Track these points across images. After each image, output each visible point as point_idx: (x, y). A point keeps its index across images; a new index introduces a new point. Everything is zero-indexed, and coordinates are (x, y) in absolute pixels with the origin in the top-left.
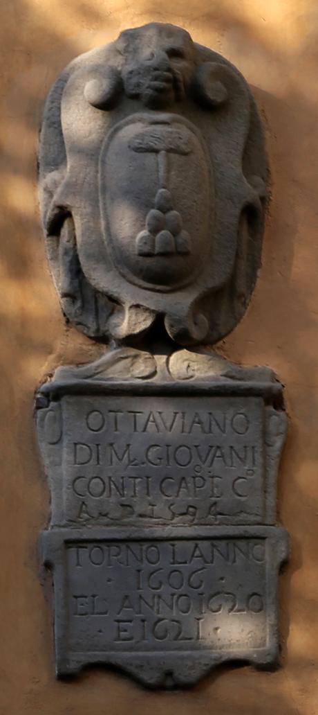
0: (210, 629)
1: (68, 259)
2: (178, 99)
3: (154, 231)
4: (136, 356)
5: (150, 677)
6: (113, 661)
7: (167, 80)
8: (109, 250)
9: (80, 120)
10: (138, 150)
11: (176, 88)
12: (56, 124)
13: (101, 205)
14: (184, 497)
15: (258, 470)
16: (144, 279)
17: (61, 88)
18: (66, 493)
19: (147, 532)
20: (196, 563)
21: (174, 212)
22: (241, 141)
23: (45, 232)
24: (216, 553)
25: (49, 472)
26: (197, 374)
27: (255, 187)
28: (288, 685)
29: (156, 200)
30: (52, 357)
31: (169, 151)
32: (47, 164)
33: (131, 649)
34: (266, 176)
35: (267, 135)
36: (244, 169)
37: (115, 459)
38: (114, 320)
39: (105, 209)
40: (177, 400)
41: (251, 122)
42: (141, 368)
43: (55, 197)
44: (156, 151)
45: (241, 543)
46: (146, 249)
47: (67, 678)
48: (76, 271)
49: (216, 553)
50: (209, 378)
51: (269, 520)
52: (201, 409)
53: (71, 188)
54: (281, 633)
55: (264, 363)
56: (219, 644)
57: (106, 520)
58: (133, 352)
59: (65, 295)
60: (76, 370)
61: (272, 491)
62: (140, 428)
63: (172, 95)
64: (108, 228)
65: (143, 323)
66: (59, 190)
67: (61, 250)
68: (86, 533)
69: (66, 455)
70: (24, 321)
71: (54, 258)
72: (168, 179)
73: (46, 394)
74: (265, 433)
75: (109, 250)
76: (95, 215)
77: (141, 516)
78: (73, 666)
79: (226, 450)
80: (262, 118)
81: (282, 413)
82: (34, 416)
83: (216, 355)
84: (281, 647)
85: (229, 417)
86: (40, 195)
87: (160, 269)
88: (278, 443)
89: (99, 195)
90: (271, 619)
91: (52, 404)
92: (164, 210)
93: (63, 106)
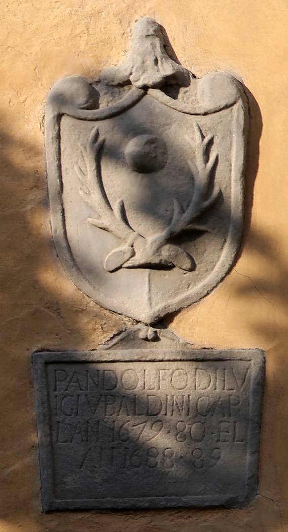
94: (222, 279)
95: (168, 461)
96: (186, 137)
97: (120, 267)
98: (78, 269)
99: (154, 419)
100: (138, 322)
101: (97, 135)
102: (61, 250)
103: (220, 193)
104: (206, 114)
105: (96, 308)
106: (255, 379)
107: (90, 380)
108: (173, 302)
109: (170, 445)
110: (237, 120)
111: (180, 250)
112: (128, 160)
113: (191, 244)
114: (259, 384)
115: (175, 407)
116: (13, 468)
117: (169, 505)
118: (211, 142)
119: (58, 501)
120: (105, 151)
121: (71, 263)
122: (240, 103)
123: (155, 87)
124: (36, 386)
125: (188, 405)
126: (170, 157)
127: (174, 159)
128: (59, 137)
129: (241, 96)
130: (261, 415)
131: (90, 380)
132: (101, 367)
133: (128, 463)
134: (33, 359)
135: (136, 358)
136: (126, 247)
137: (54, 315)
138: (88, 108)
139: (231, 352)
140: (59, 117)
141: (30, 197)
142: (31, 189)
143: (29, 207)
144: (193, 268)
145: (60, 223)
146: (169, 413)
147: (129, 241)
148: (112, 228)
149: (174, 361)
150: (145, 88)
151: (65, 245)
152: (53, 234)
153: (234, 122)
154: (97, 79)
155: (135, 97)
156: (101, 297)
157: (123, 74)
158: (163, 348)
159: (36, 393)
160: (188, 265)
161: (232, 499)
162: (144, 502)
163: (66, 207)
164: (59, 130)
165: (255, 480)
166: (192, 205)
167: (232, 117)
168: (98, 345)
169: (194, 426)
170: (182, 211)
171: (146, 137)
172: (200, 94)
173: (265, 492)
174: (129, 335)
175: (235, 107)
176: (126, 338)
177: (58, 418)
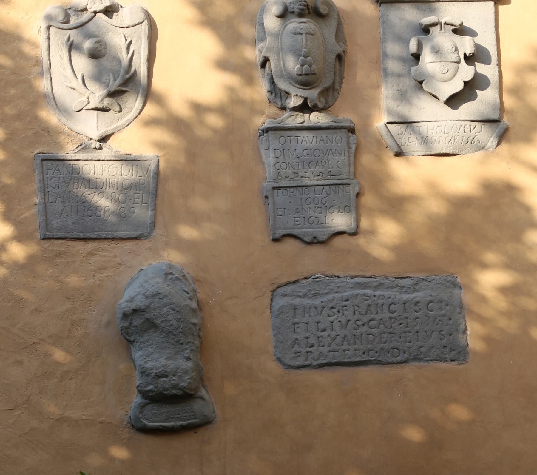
0: (330, 220)
1: (269, 77)
2: (309, 13)
3: (302, 65)
4: (297, 115)
5: (308, 239)
6: (293, 233)
7: (305, 6)
8: (285, 74)
9: (271, 22)
10: (295, 33)
11: (308, 9)
12: (262, 24)
13: (281, 55)
14: (318, 169)
15: (346, 158)
16: (299, 84)
17: (263, 10)
18: (272, 169)
19: (304, 183)
20: (324, 195)
21: (310, 58)
22: (335, 29)
23: (260, 67)
24: (331, 191)
25: (265, 161)
26: (321, 121)
27: (341, 47)
28: (361, 240)
29: (302, 53)
30: (264, 116)
31: (307, 33)
32: (259, 40)
33: (300, 228)
34: (345, 42)
35: (345, 26)
36: (336, 40)
37: (290, 155)
38: (288, 101)
39: (282, 57)
40: (314, 131)
41: (338, 21)
42: (299, 119)
43: (263, 53)
44: (302, 34)
45: (341, 187)
46: (299, 73)
47: (276, 240)
48: (272, 82)
49: (331, 191)
50: (325, 123)
51: (351, 177)
52: (323, 134)
53: (269, 49)
54: (358, 221)
55: (347, 116)
56: (334, 225)
57: (288, 179)
58: (296, 113)
59: (268, 92)
60: (274, 121)
61: (352, 166)
62: (300, 143)
63: (307, 11)
64: (284, 65)
65: (300, 102)
66: (264, 50)
67: (266, 74)
68: (281, 184)
69: (271, 154)
70: (253, 102)
71: (263, 77)
72: (306, 45)
73: (263, 131)
74: (348, 143)
75: (285, 74)
76: (279, 60)
77: (301, 177)
78: (278, 236)
79: (333, 150)
80: (342, 20)
81: (355, 136)
82: (258, 139)
83: (328, 114)
84: (358, 226)
85: (334, 137)
86: (257, 52)
87: (305, 81)
88: (354, 147)
89: (280, 51)
90: (354, 215)
91: (265, 134)
92: (305, 57)
93: (264, 17)
94: (136, 117)
95: (107, 213)
96: (116, 40)
97: (82, 110)
98: (59, 110)
99: (100, 191)
100: (91, 139)
101: (69, 37)
102: (50, 99)
103: (135, 71)
104: (127, 27)
105: (69, 131)
106: (153, 171)
107: (66, 170)
108: (109, 129)
109: (108, 205)
110: (145, 31)
111: (114, 101)
112: (86, 52)
113: (119, 97)
114: (155, 174)
115: (111, 185)
116: (24, 215)
117: (107, 237)
118: (130, 43)
119: (48, 233)
120: (73, 46)
121: (55, 107)
122: (146, 22)
123: (100, 12)
124: (37, 172)
125: (118, 184)
126: (108, 50)
127: (110, 51)
128: (49, 38)
129: (147, 18)
130: (156, 190)
131: (66, 170)
132: (71, 162)
133: (86, 214)
134: (35, 158)
135: (90, 158)
136: (85, 99)
137: (46, 135)
138: (64, 23)
139: (141, 156)
140: (49, 27)
141: (34, 70)
142: (34, 66)
143: (33, 76)
144: (120, 111)
145: (50, 85)
146: (107, 188)
147: (87, 96)
148: (76, 88)
149: (110, 160)
150: (95, 13)
151: (52, 97)
152: (46, 91)
153: (143, 32)
154: (69, 7)
155: (90, 17)
156: (71, 125)
157: (82, 5)
158: (104, 154)
159: (37, 176)
160: (118, 109)
161: (141, 234)
162: (94, 235)
163: (53, 76)
164: (49, 34)
165: (153, 224)
166: (120, 77)
167: (142, 29)
168: (70, 151)
169: (121, 195)
170: (115, 80)
171: (95, 39)
172: (124, 17)
173: (158, 231)
174: (86, 146)
175: (143, 24)
176: (84, 147)
177: (48, 190)
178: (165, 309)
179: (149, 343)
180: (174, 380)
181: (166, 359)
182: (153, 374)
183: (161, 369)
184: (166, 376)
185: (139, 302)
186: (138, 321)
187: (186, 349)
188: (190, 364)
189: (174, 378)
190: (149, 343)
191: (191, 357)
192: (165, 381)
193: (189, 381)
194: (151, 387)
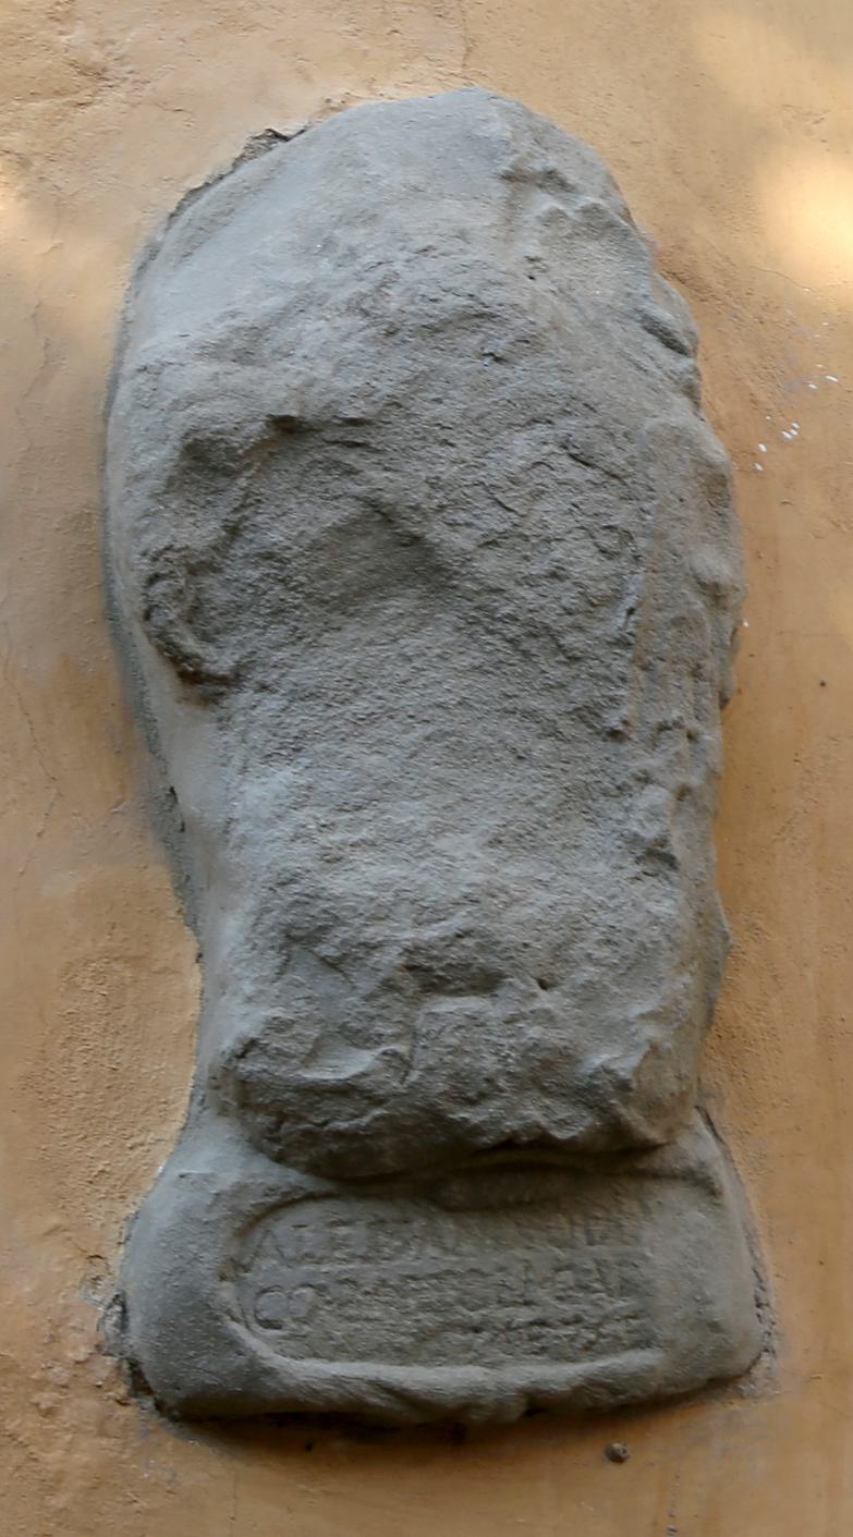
178: (521, 446)
179: (361, 706)
180: (548, 1018)
181: (496, 842)
182: (391, 958)
183: (459, 921)
184: (488, 983)
185: (319, 366)
186: (297, 515)
187: (645, 779)
188: (665, 903)
189: (546, 1001)
190: (361, 706)
191: (677, 849)
192: (475, 1020)
193: (651, 1031)
194: (355, 1064)
